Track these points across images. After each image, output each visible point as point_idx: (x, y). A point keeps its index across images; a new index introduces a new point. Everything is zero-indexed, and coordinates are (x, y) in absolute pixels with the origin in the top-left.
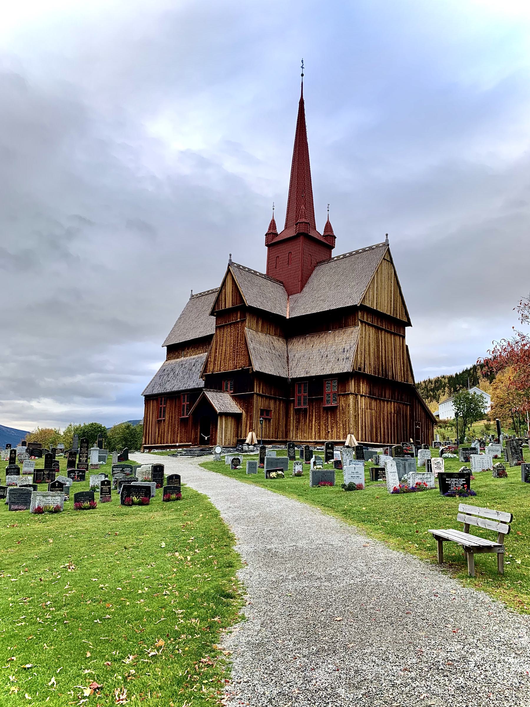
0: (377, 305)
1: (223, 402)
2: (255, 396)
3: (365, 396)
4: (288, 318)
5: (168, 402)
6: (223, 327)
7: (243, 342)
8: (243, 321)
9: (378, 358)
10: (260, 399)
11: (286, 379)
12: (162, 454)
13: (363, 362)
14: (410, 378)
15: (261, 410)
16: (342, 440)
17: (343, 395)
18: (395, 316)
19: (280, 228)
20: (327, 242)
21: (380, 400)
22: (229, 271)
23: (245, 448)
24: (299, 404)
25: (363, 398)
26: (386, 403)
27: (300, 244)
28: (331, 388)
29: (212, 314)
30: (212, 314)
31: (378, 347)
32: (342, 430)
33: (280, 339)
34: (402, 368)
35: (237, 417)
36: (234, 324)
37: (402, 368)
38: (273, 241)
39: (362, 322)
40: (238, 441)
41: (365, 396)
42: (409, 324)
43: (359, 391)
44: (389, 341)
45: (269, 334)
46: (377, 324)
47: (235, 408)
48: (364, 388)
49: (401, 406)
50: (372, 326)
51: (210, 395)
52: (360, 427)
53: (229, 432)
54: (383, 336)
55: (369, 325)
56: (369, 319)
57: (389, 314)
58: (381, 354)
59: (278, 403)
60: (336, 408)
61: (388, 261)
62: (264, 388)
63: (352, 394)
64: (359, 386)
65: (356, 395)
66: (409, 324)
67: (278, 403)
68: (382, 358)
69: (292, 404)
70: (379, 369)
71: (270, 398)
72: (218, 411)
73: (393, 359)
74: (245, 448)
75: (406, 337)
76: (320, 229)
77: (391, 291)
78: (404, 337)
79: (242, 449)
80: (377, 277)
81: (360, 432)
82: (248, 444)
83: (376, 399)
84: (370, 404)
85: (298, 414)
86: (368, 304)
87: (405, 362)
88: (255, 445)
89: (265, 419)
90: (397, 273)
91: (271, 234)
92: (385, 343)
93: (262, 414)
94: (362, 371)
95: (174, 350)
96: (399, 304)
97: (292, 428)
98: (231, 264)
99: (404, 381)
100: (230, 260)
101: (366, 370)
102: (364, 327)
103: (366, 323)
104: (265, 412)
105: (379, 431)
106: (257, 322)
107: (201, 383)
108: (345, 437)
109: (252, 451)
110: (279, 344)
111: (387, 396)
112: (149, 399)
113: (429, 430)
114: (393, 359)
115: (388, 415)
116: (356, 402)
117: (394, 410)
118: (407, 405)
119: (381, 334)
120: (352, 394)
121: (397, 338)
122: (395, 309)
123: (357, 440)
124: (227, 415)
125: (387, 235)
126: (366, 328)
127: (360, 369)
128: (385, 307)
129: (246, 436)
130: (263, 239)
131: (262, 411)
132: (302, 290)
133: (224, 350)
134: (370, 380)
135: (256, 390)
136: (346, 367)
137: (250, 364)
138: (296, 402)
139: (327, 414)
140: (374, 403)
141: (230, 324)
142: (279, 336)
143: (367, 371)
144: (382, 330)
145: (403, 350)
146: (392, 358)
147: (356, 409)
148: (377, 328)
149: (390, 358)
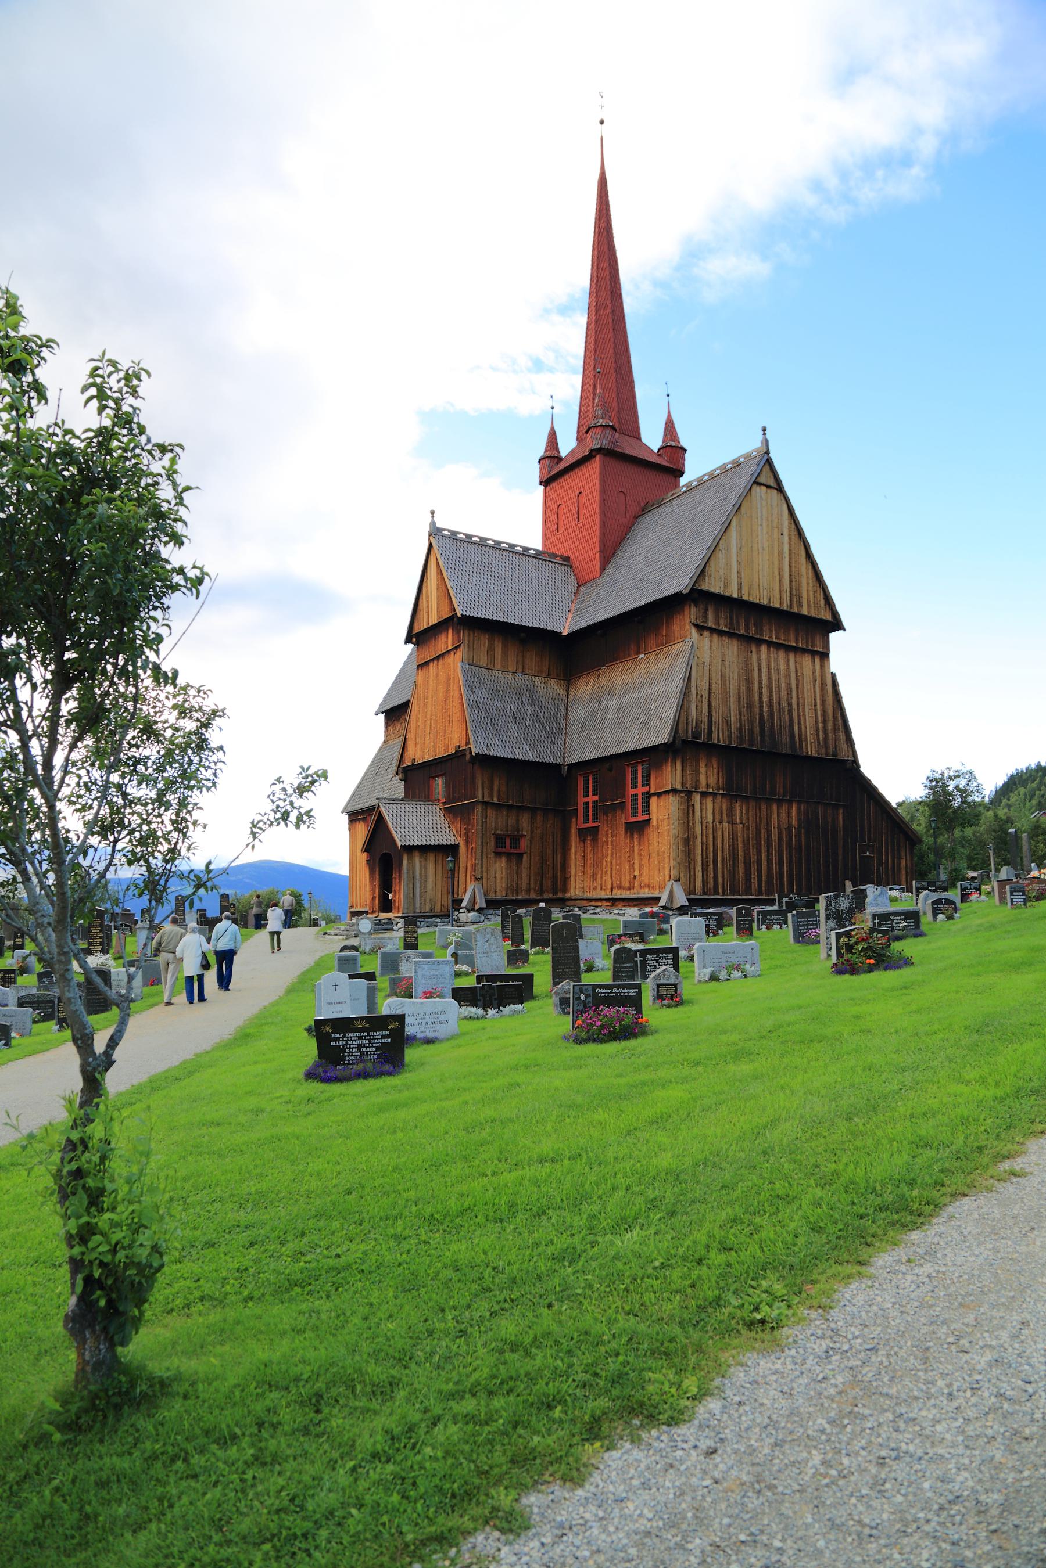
0: (740, 589)
2: (479, 809)
3: (714, 795)
4: (565, 633)
6: (427, 663)
7: (457, 694)
9: (750, 706)
11: (557, 767)
13: (705, 719)
14: (844, 746)
15: (496, 835)
16: (656, 894)
17: (659, 795)
18: (795, 610)
21: (757, 799)
23: (463, 916)
24: (586, 820)
25: (709, 800)
26: (775, 807)
27: (612, 465)
31: (749, 681)
32: (656, 872)
34: (820, 725)
36: (443, 655)
37: (820, 725)
38: (555, 471)
39: (700, 628)
41: (714, 795)
42: (837, 625)
43: (697, 786)
44: (783, 667)
45: (523, 672)
46: (747, 630)
47: (446, 836)
48: (709, 775)
49: (820, 810)
50: (730, 635)
52: (700, 863)
53: (430, 885)
54: (764, 656)
55: (721, 633)
56: (722, 622)
57: (777, 605)
58: (757, 698)
59: (539, 818)
61: (768, 487)
62: (503, 789)
63: (674, 791)
64: (696, 772)
65: (689, 794)
66: (837, 625)
67: (539, 818)
68: (761, 707)
70: (751, 731)
71: (520, 809)
72: (399, 844)
73: (795, 706)
75: (831, 655)
77: (780, 554)
78: (825, 655)
80: (739, 525)
81: (699, 875)
83: (746, 798)
86: (713, 585)
87: (830, 712)
89: (509, 855)
90: (798, 513)
92: (769, 672)
94: (703, 739)
99: (827, 754)
101: (714, 735)
103: (712, 630)
105: (754, 868)
106: (491, 649)
108: (661, 888)
109: (473, 923)
110: (550, 689)
111: (779, 789)
113: (900, 858)
114: (795, 706)
115: (780, 833)
116: (688, 810)
117: (799, 820)
118: (837, 806)
119: (759, 652)
120: (674, 791)
122: (795, 594)
123: (690, 891)
125: (764, 430)
126: (711, 641)
131: (500, 840)
133: (429, 713)
136: (659, 734)
137: (468, 743)
141: (438, 658)
142: (549, 676)
143: (719, 737)
144: (759, 642)
145: (823, 685)
146: (790, 704)
148: (747, 640)
149: (784, 703)
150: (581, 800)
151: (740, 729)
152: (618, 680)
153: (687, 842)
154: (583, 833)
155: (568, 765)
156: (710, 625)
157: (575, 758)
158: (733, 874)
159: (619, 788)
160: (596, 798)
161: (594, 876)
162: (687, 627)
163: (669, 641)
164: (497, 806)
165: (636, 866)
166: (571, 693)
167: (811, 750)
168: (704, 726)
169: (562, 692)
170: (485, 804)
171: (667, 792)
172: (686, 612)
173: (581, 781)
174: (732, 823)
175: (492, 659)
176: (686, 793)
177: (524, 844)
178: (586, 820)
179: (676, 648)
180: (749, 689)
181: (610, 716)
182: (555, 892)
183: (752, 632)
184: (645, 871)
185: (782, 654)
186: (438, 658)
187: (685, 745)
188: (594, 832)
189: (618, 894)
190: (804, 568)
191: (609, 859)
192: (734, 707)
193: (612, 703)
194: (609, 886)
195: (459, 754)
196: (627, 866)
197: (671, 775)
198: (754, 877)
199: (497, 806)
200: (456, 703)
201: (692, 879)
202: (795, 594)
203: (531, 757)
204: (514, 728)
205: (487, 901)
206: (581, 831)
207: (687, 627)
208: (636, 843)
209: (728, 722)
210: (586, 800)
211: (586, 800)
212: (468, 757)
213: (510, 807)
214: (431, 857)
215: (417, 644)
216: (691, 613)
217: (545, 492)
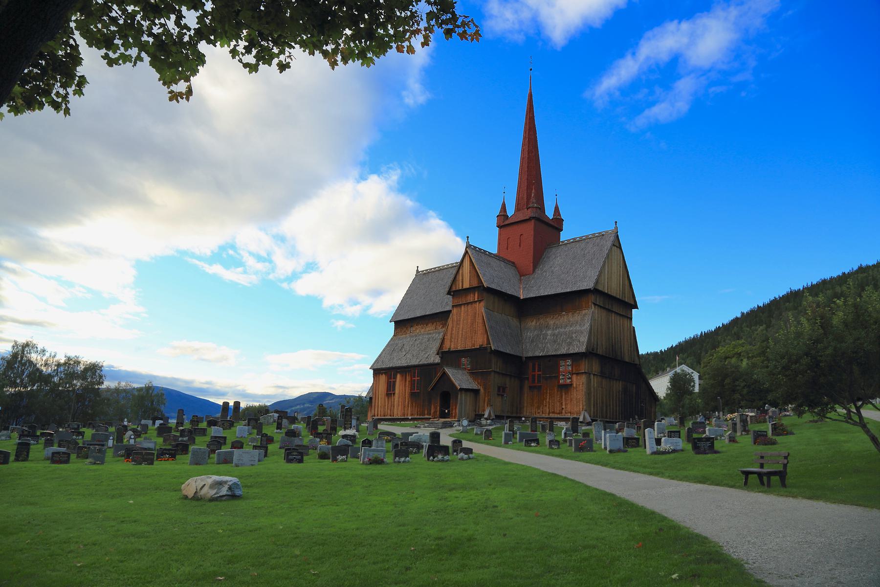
1: (460, 378)
5: (398, 376)
7: (481, 321)
8: (480, 301)
11: (521, 357)
12: (398, 425)
17: (577, 374)
19: (510, 212)
20: (557, 225)
22: (466, 252)
23: (484, 422)
28: (566, 366)
29: (449, 293)
30: (449, 293)
36: (471, 303)
39: (595, 304)
42: (636, 307)
48: (596, 367)
50: (604, 308)
51: (450, 371)
66: (636, 307)
69: (527, 382)
74: (484, 422)
76: (550, 213)
78: (631, 319)
82: (487, 419)
86: (600, 288)
91: (503, 215)
95: (402, 324)
96: (627, 287)
98: (468, 246)
100: (468, 243)
104: (501, 391)
107: (437, 360)
110: (514, 322)
112: (377, 372)
121: (626, 320)
122: (624, 293)
124: (467, 390)
128: (613, 288)
129: (484, 411)
130: (495, 221)
131: (499, 388)
132: (534, 271)
134: (604, 359)
137: (489, 343)
141: (468, 304)
143: (600, 352)
148: (609, 310)
152: (551, 322)
157: (530, 354)
161: (538, 408)
164: (498, 373)
167: (627, 359)
173: (531, 364)
179: (584, 312)
181: (548, 337)
183: (610, 308)
184: (569, 406)
185: (618, 317)
186: (468, 304)
187: (589, 354)
189: (552, 415)
190: (627, 282)
193: (549, 332)
195: (481, 350)
199: (498, 373)
200: (481, 325)
202: (624, 293)
203: (512, 353)
206: (530, 387)
215: (453, 296)
216: (592, 298)
217: (500, 234)
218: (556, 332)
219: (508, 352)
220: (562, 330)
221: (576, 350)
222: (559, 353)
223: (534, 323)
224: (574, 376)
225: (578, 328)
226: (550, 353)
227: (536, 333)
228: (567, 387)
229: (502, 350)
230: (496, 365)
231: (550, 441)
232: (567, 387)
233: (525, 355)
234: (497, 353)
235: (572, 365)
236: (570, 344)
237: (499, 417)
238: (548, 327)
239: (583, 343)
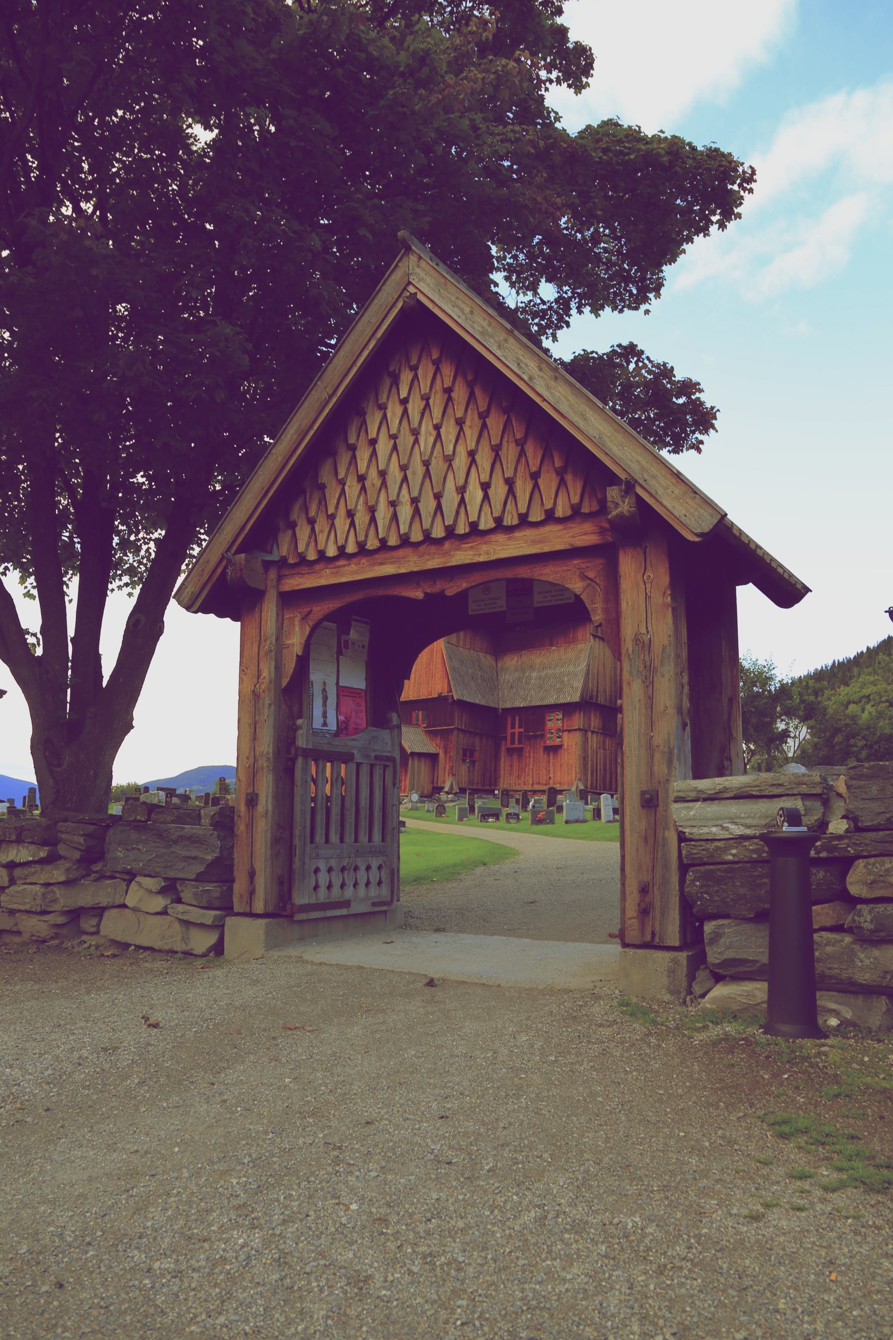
2: (456, 732)
3: (597, 733)
7: (439, 661)
9: (615, 683)
10: (461, 735)
11: (495, 710)
13: (595, 689)
17: (569, 731)
23: (443, 796)
24: (513, 742)
28: (554, 722)
33: (488, 656)
35: (433, 758)
39: (595, 636)
40: (434, 788)
41: (597, 733)
47: (429, 746)
60: (560, 747)
63: (579, 729)
64: (590, 719)
65: (586, 731)
72: (409, 751)
79: (440, 799)
81: (589, 777)
82: (448, 793)
84: (604, 742)
85: (511, 756)
88: (455, 794)
93: (464, 755)
97: (502, 774)
102: (597, 644)
109: (452, 801)
110: (487, 660)
116: (585, 741)
120: (579, 729)
124: (420, 755)
127: (591, 698)
131: (465, 751)
135: (457, 724)
136: (576, 698)
138: (509, 738)
139: (549, 755)
140: (607, 740)
142: (486, 653)
143: (601, 700)
147: (585, 750)
150: (510, 731)
151: (611, 696)
153: (585, 758)
154: (510, 751)
155: (503, 709)
156: (599, 634)
157: (508, 705)
158: (604, 778)
159: (541, 724)
160: (522, 730)
161: (519, 777)
162: (588, 635)
163: (574, 641)
164: (464, 731)
165: (551, 772)
166: (499, 665)
168: (595, 693)
169: (494, 663)
170: (459, 730)
171: (576, 730)
172: (588, 627)
174: (604, 749)
175: (458, 641)
176: (584, 731)
177: (477, 755)
178: (513, 742)
179: (580, 646)
180: (615, 673)
181: (533, 681)
182: (490, 785)
184: (558, 774)
188: (520, 751)
189: (536, 787)
191: (531, 766)
192: (608, 683)
193: (534, 674)
194: (531, 783)
196: (545, 772)
197: (578, 720)
198: (614, 781)
200: (439, 666)
201: (587, 780)
203: (483, 703)
204: (473, 684)
205: (460, 789)
207: (588, 635)
208: (551, 758)
209: (605, 691)
210: (513, 731)
211: (513, 731)
212: (450, 701)
213: (470, 733)
214: (423, 760)
218: (543, 673)
219: (477, 702)
220: (550, 672)
221: (568, 700)
222: (546, 702)
223: (514, 662)
224: (566, 733)
225: (572, 669)
226: (534, 703)
227: (517, 675)
228: (555, 749)
229: (468, 700)
230: (459, 721)
231: (507, 815)
232: (555, 749)
233: (501, 706)
234: (461, 703)
235: (563, 719)
236: (560, 691)
237: (462, 791)
238: (532, 667)
239: (577, 689)
